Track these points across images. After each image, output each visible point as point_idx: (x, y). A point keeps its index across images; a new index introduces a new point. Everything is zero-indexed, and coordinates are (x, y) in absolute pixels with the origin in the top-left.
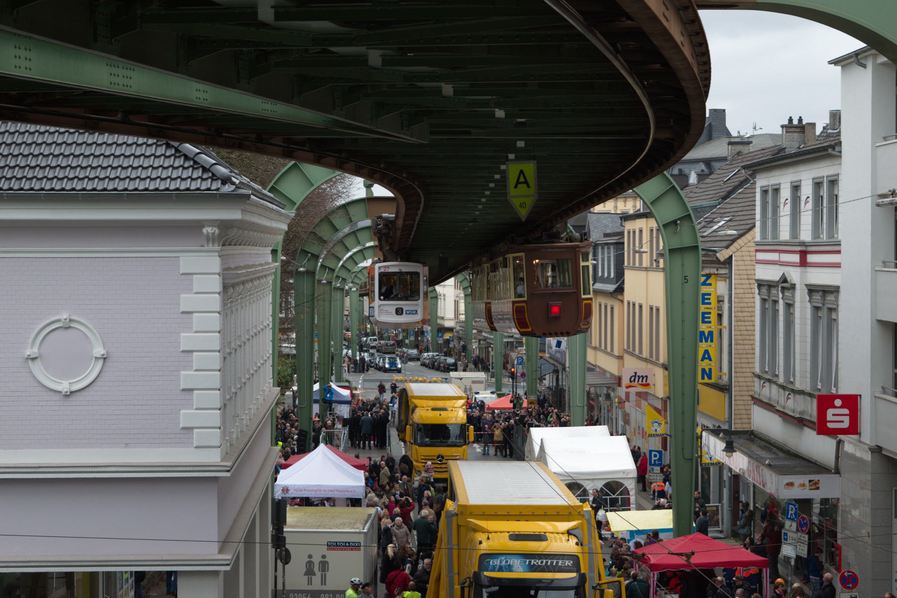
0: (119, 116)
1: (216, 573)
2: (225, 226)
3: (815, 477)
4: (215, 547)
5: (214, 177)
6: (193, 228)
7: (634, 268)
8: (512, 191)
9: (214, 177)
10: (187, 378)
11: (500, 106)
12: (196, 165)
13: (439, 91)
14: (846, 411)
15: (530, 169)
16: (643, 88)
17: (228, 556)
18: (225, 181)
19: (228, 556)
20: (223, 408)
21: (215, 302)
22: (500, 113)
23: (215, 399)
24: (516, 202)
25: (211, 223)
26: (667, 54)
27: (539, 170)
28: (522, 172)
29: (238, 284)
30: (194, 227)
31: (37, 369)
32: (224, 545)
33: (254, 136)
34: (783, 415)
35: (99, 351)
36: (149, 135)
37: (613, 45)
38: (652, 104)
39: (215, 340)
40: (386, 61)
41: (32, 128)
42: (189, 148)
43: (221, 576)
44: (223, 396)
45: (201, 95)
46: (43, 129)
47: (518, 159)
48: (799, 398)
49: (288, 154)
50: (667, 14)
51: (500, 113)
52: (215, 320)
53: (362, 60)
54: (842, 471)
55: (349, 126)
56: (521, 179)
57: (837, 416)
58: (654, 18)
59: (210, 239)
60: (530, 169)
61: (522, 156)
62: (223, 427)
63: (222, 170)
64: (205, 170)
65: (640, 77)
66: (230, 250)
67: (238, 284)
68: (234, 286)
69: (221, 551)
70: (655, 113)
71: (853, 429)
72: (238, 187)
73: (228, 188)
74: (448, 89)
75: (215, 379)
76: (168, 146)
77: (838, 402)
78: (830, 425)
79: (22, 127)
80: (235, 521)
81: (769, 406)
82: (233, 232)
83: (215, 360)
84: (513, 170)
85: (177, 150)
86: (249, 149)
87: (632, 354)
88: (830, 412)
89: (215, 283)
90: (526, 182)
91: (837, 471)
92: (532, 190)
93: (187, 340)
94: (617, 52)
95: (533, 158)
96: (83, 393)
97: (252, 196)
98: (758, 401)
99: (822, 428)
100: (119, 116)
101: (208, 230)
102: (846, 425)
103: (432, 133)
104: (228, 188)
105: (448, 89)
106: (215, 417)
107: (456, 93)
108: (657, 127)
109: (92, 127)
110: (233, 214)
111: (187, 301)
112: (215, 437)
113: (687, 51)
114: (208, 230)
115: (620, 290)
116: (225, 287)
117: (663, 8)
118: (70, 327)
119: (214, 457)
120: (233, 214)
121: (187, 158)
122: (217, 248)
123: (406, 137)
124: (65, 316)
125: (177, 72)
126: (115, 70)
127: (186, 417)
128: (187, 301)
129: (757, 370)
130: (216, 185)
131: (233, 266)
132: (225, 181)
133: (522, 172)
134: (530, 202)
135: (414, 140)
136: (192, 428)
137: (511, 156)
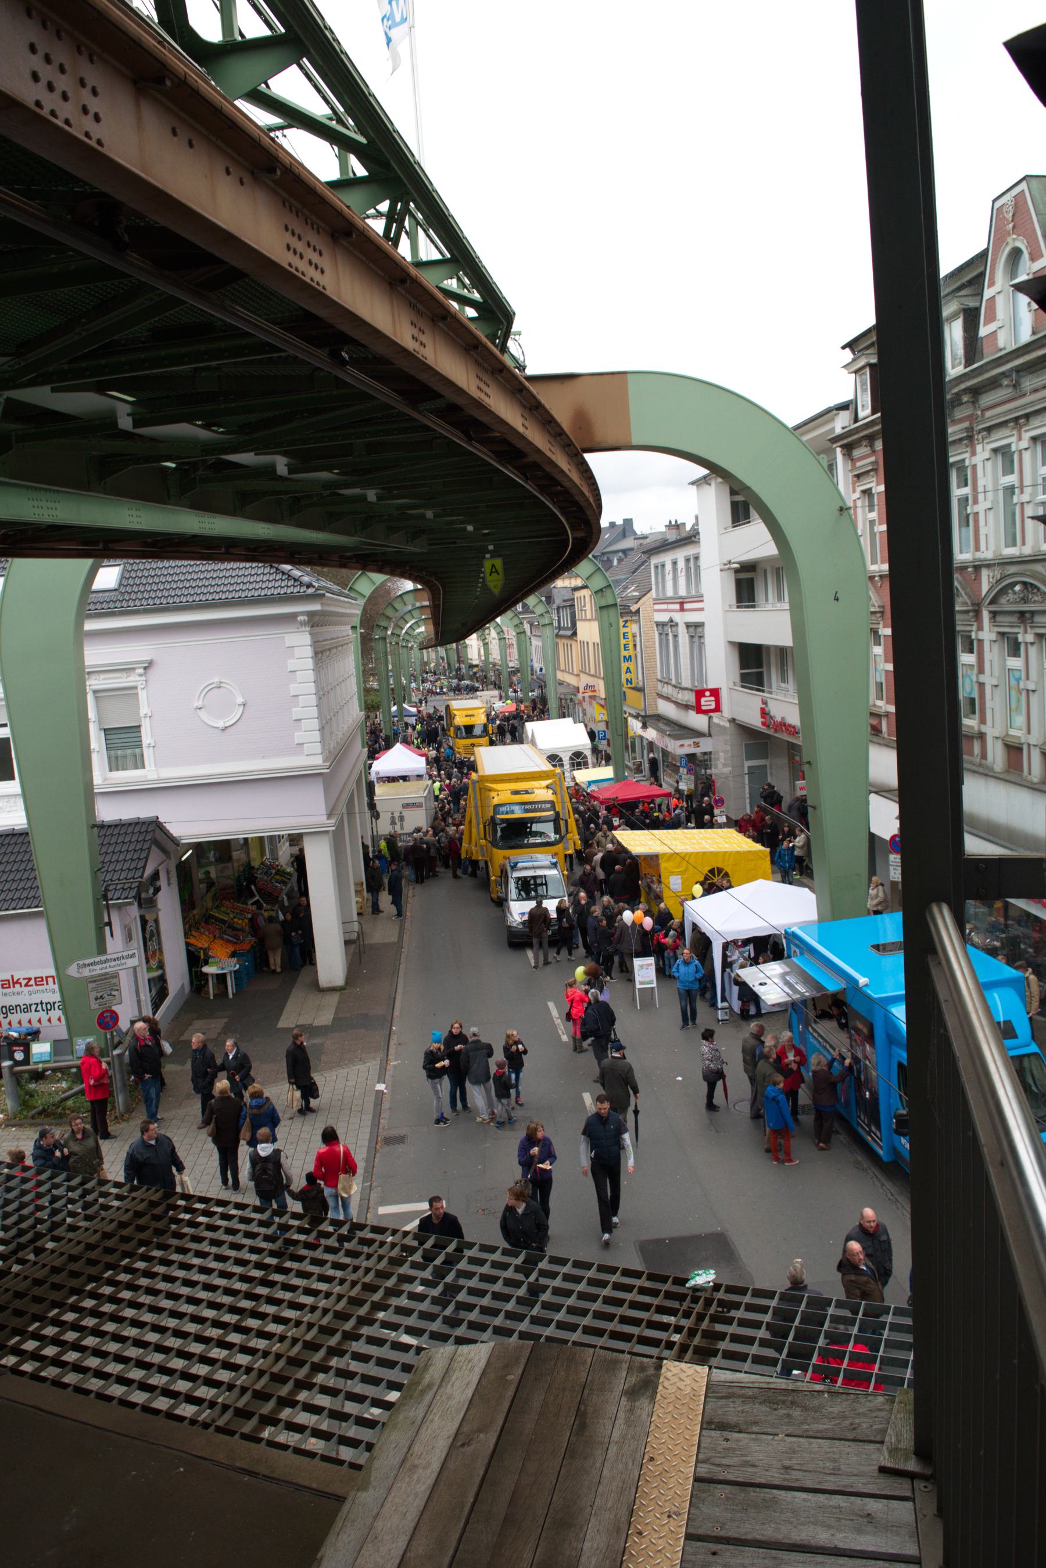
0: (223, 550)
1: (327, 832)
2: (311, 614)
3: (696, 740)
4: (325, 817)
5: (301, 584)
6: (291, 617)
7: (582, 620)
8: (488, 578)
9: (301, 584)
10: (297, 712)
11: (469, 523)
12: (290, 577)
13: (423, 516)
14: (713, 698)
15: (498, 563)
16: (554, 503)
17: (333, 821)
18: (309, 586)
19: (333, 821)
20: (322, 729)
21: (309, 663)
22: (470, 528)
23: (315, 724)
24: (491, 585)
25: (303, 613)
26: (558, 477)
27: (504, 563)
28: (493, 565)
29: (325, 651)
30: (291, 617)
31: (202, 714)
32: (330, 816)
33: (316, 556)
34: (676, 703)
35: (240, 700)
36: (247, 560)
37: (524, 474)
38: (562, 514)
39: (311, 688)
40: (379, 498)
41: (186, 563)
42: (287, 567)
43: (331, 834)
44: (321, 723)
45: (266, 531)
46: (192, 563)
47: (492, 557)
48: (686, 692)
49: (344, 566)
50: (553, 449)
51: (470, 528)
52: (310, 675)
53: (363, 499)
54: (712, 732)
55: (371, 544)
56: (494, 570)
57: (707, 702)
58: (538, 451)
59: (303, 624)
60: (498, 563)
61: (495, 555)
62: (323, 741)
63: (306, 579)
64: (295, 580)
65: (551, 496)
66: (317, 630)
67: (325, 651)
68: (322, 652)
69: (328, 819)
70: (567, 520)
71: (718, 709)
72: (317, 590)
73: (311, 591)
74: (430, 514)
75: (314, 712)
76: (271, 567)
77: (707, 693)
78: (704, 708)
79: (179, 563)
80: (338, 798)
81: (667, 699)
82: (316, 618)
83: (313, 700)
84: (487, 565)
85: (277, 569)
86: (315, 564)
87: (585, 673)
88: (703, 700)
89: (309, 652)
90: (497, 572)
91: (710, 735)
92: (501, 576)
93: (294, 689)
94: (526, 479)
95: (500, 556)
96: (234, 727)
97: (327, 595)
98: (661, 696)
99: (699, 710)
100: (223, 550)
101: (301, 618)
102: (713, 706)
103: (430, 545)
104: (311, 591)
105: (430, 514)
106: (316, 736)
107: (435, 516)
108: (572, 530)
109: (221, 559)
110: (316, 607)
111: (292, 664)
112: (318, 748)
113: (575, 476)
114: (301, 618)
115: (575, 634)
116: (316, 653)
117: (549, 445)
118: (219, 687)
119: (318, 760)
120: (316, 607)
121: (283, 573)
122: (308, 629)
123: (411, 549)
124: (216, 680)
125: (234, 515)
126: (202, 519)
127: (298, 737)
128: (292, 664)
129: (659, 677)
130: (303, 589)
131: (321, 639)
132: (309, 586)
133: (493, 565)
134: (500, 584)
135: (417, 550)
136: (302, 744)
137: (488, 556)
